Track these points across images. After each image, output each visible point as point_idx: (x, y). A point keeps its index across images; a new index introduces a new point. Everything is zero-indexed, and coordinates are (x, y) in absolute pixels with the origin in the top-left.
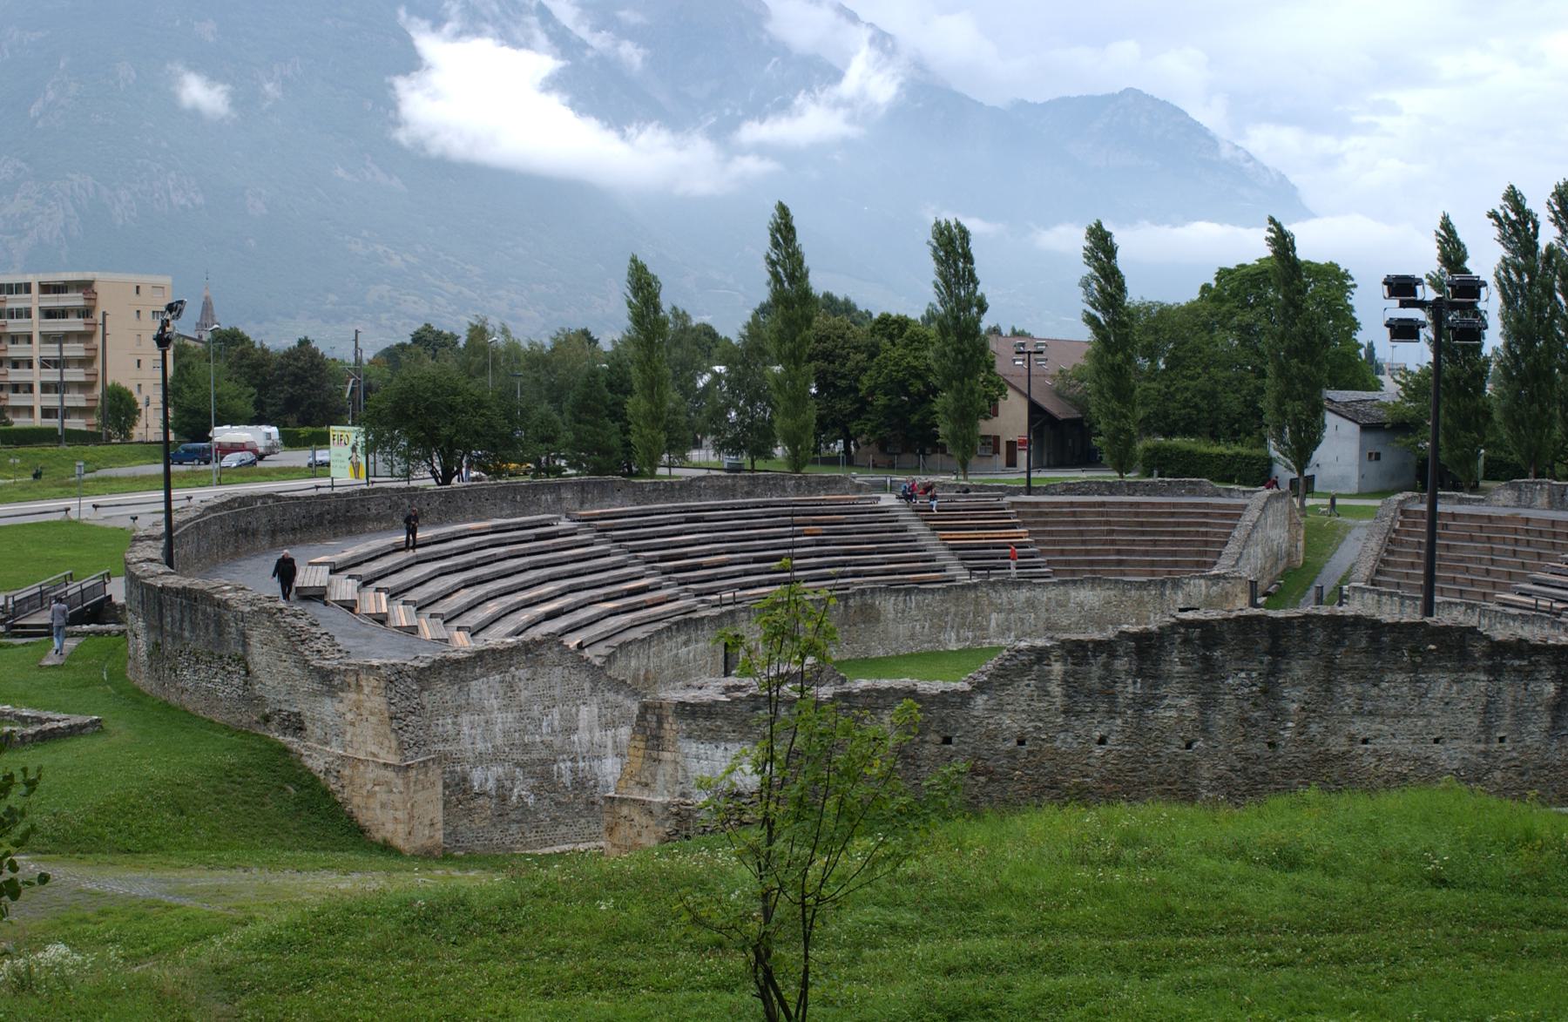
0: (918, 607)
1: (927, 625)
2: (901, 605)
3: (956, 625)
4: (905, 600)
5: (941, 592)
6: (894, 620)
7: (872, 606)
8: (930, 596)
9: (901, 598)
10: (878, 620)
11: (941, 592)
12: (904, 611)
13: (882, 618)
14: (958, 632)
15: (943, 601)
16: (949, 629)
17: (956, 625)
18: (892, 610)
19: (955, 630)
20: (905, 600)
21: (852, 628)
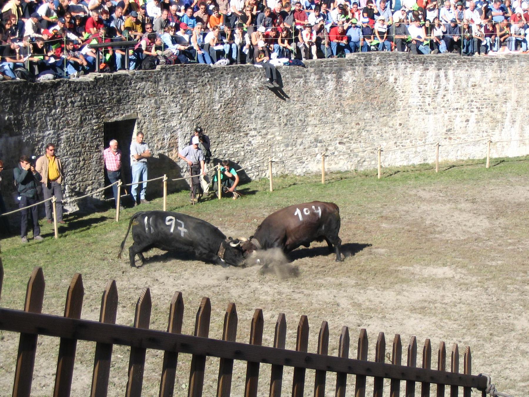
0: (458, 88)
1: (473, 118)
2: (431, 87)
3: (518, 119)
4: (438, 76)
5: (495, 64)
6: (420, 108)
7: (382, 84)
8: (477, 73)
9: (432, 72)
10: (393, 109)
11: (495, 64)
13: (400, 104)
14: (522, 128)
15: (500, 81)
16: (507, 122)
17: (518, 119)
19: (517, 125)
20: (438, 76)
21: (348, 118)
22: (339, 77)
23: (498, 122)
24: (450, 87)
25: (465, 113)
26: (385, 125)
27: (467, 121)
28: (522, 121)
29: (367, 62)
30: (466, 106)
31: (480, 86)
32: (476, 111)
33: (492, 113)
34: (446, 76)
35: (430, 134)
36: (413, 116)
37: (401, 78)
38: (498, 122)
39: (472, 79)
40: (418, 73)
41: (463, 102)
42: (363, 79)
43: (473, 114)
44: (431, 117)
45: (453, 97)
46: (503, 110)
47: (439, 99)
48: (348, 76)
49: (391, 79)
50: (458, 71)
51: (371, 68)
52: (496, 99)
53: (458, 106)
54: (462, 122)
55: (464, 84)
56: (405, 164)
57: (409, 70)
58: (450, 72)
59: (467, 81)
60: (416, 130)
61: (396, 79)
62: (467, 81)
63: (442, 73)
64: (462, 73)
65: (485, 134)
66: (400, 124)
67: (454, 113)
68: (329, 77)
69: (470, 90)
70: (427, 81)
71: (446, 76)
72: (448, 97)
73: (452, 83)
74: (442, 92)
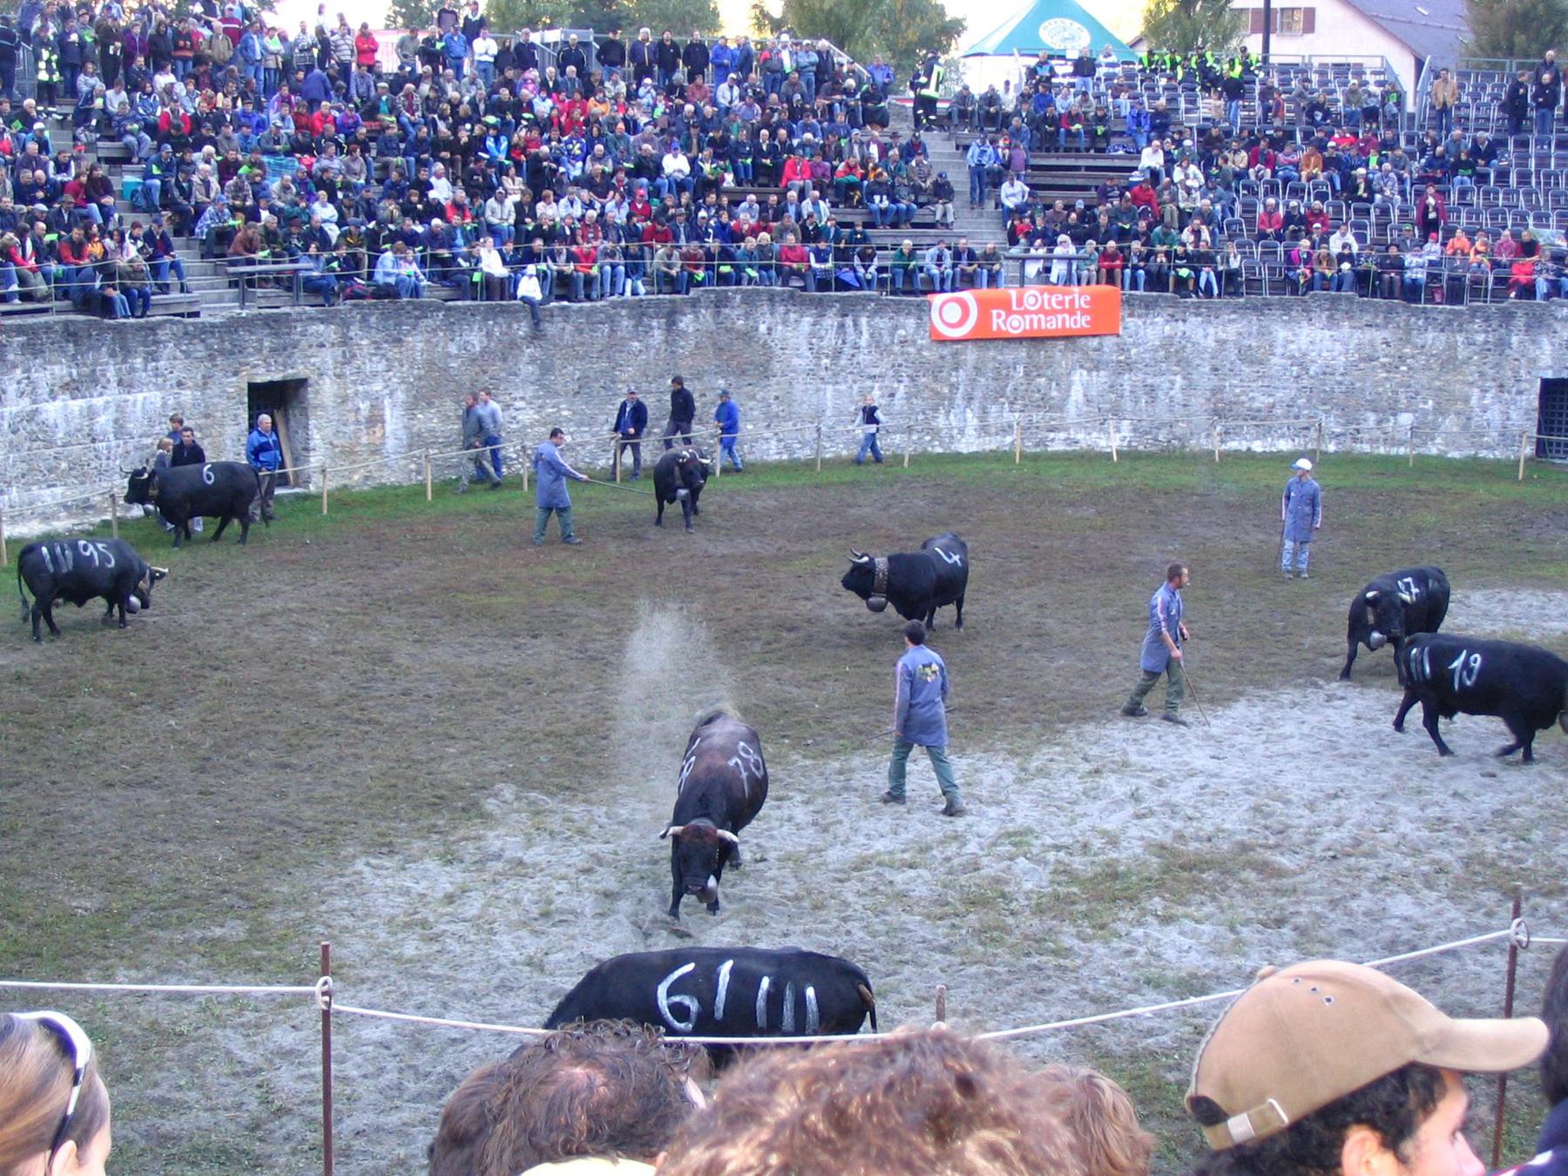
1: (901, 390)
2: (830, 339)
3: (978, 394)
4: (842, 326)
6: (811, 373)
7: (748, 336)
9: (831, 321)
12: (838, 353)
13: (776, 367)
14: (984, 411)
16: (959, 401)
17: (978, 394)
18: (804, 348)
19: (976, 404)
20: (842, 326)
22: (671, 324)
23: (944, 399)
24: (864, 340)
25: (887, 383)
26: (753, 397)
27: (892, 395)
28: (985, 398)
29: (720, 303)
30: (891, 373)
31: (914, 342)
32: (906, 380)
33: (933, 385)
34: (856, 325)
35: (828, 413)
36: (798, 387)
37: (780, 327)
38: (944, 399)
39: (902, 332)
40: (807, 320)
41: (884, 367)
42: (714, 327)
43: (902, 387)
44: (830, 387)
45: (868, 358)
46: (953, 380)
47: (843, 362)
48: (686, 322)
49: (763, 328)
50: (877, 320)
51: (727, 311)
52: (940, 363)
53: (876, 371)
54: (882, 396)
55: (886, 339)
56: (785, 457)
57: (792, 316)
58: (863, 321)
59: (892, 335)
60: (805, 406)
61: (769, 329)
62: (892, 335)
63: (849, 321)
64: (882, 323)
65: (921, 417)
66: (777, 398)
67: (869, 383)
68: (655, 323)
69: (896, 348)
70: (823, 333)
71: (856, 325)
72: (860, 357)
73: (866, 336)
74: (847, 350)
